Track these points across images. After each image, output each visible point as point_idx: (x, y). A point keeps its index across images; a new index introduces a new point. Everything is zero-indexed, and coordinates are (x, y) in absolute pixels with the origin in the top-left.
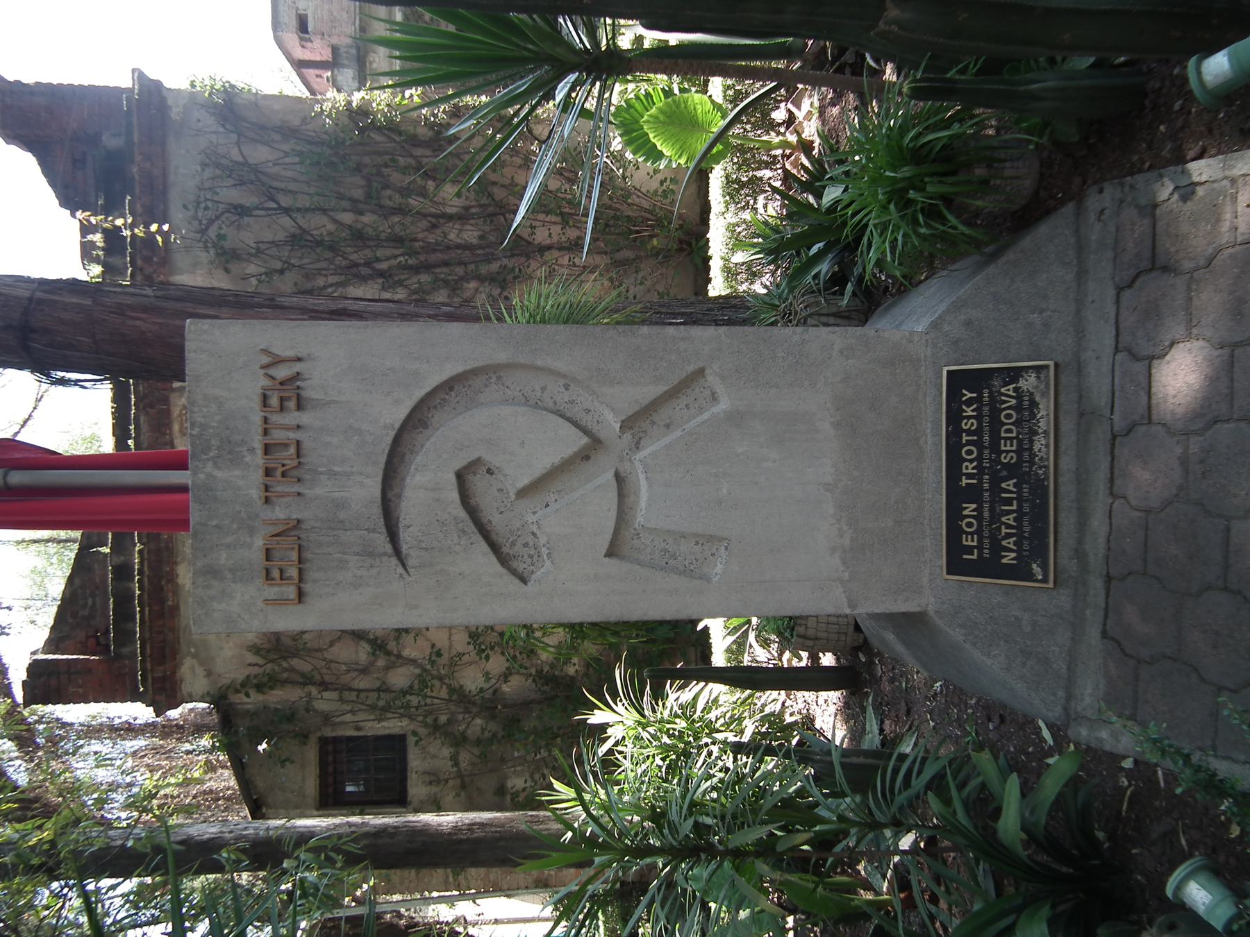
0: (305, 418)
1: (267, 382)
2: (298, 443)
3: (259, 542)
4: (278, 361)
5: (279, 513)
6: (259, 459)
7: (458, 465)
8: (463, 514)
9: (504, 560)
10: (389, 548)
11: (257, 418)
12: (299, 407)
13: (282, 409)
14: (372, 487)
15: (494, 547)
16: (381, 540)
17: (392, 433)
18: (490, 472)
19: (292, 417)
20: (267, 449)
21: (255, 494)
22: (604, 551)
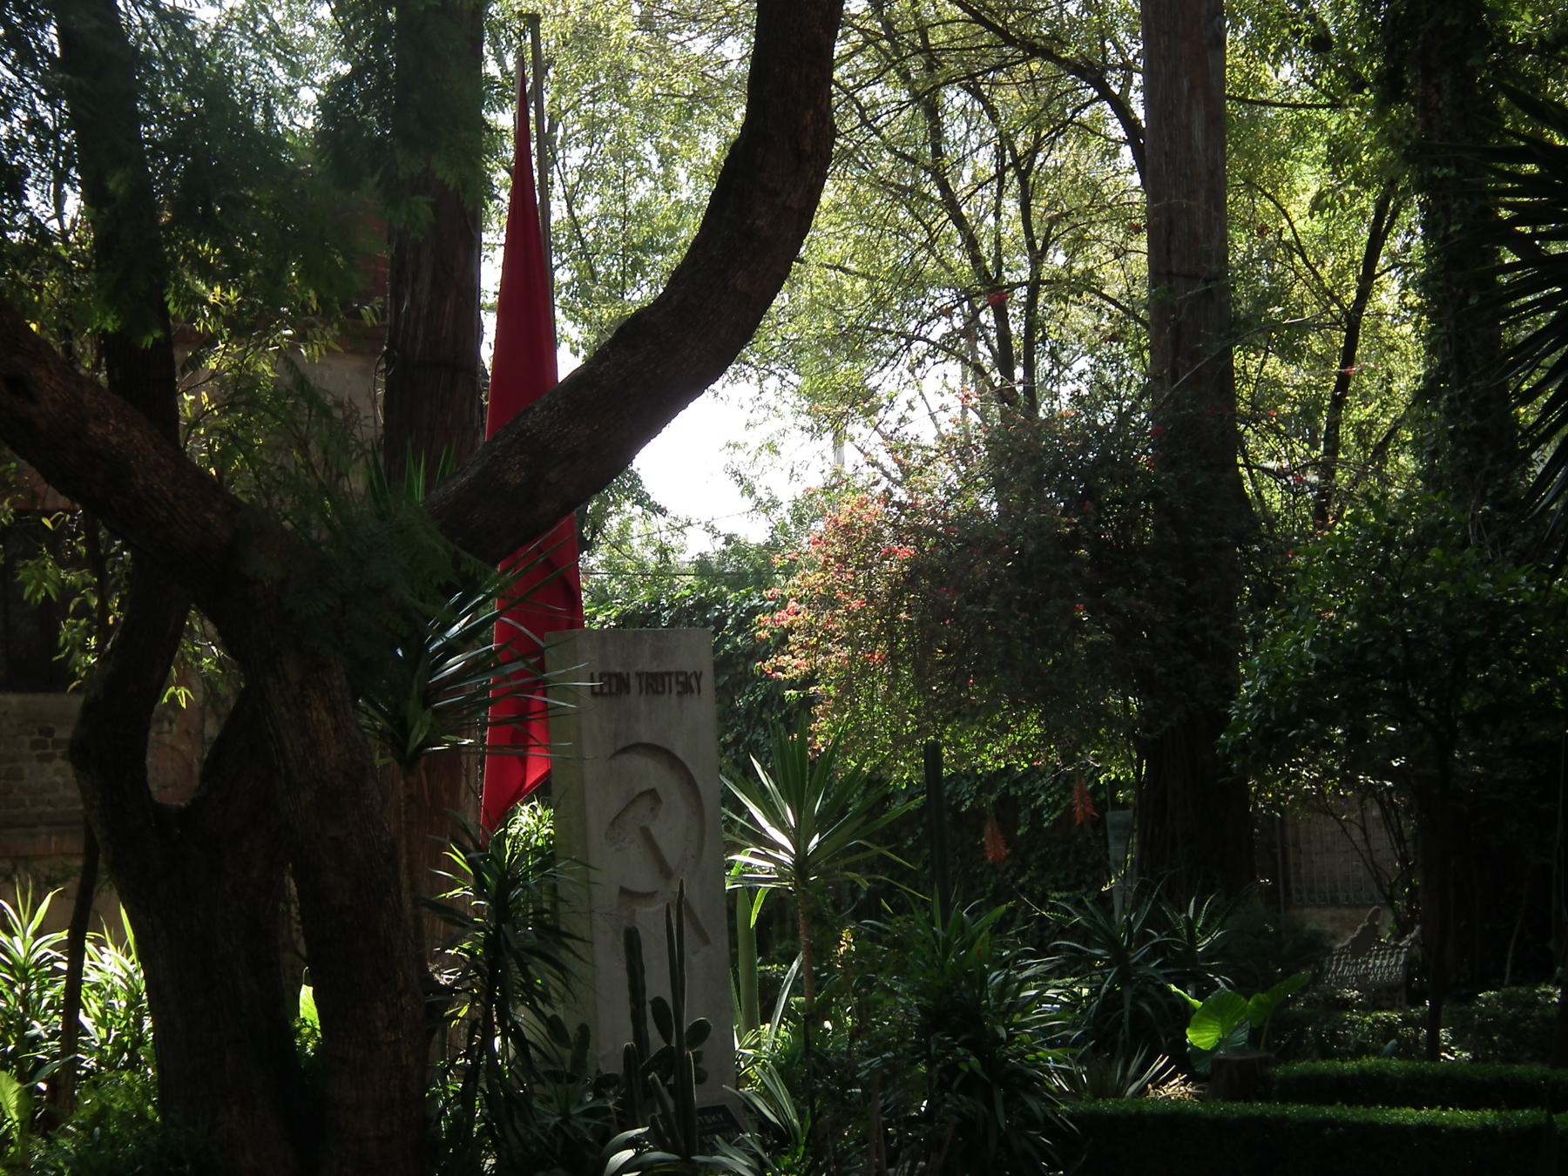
0: (674, 696)
1: (689, 672)
2: (662, 693)
3: (618, 670)
4: (698, 680)
5: (634, 682)
6: (654, 668)
7: (660, 792)
8: (637, 792)
9: (613, 823)
10: (619, 748)
11: (672, 669)
12: (679, 693)
13: (678, 682)
14: (646, 739)
15: (617, 817)
16: (622, 744)
17: (668, 747)
18: (652, 809)
19: (675, 689)
20: (662, 675)
21: (639, 668)
22: (627, 885)
